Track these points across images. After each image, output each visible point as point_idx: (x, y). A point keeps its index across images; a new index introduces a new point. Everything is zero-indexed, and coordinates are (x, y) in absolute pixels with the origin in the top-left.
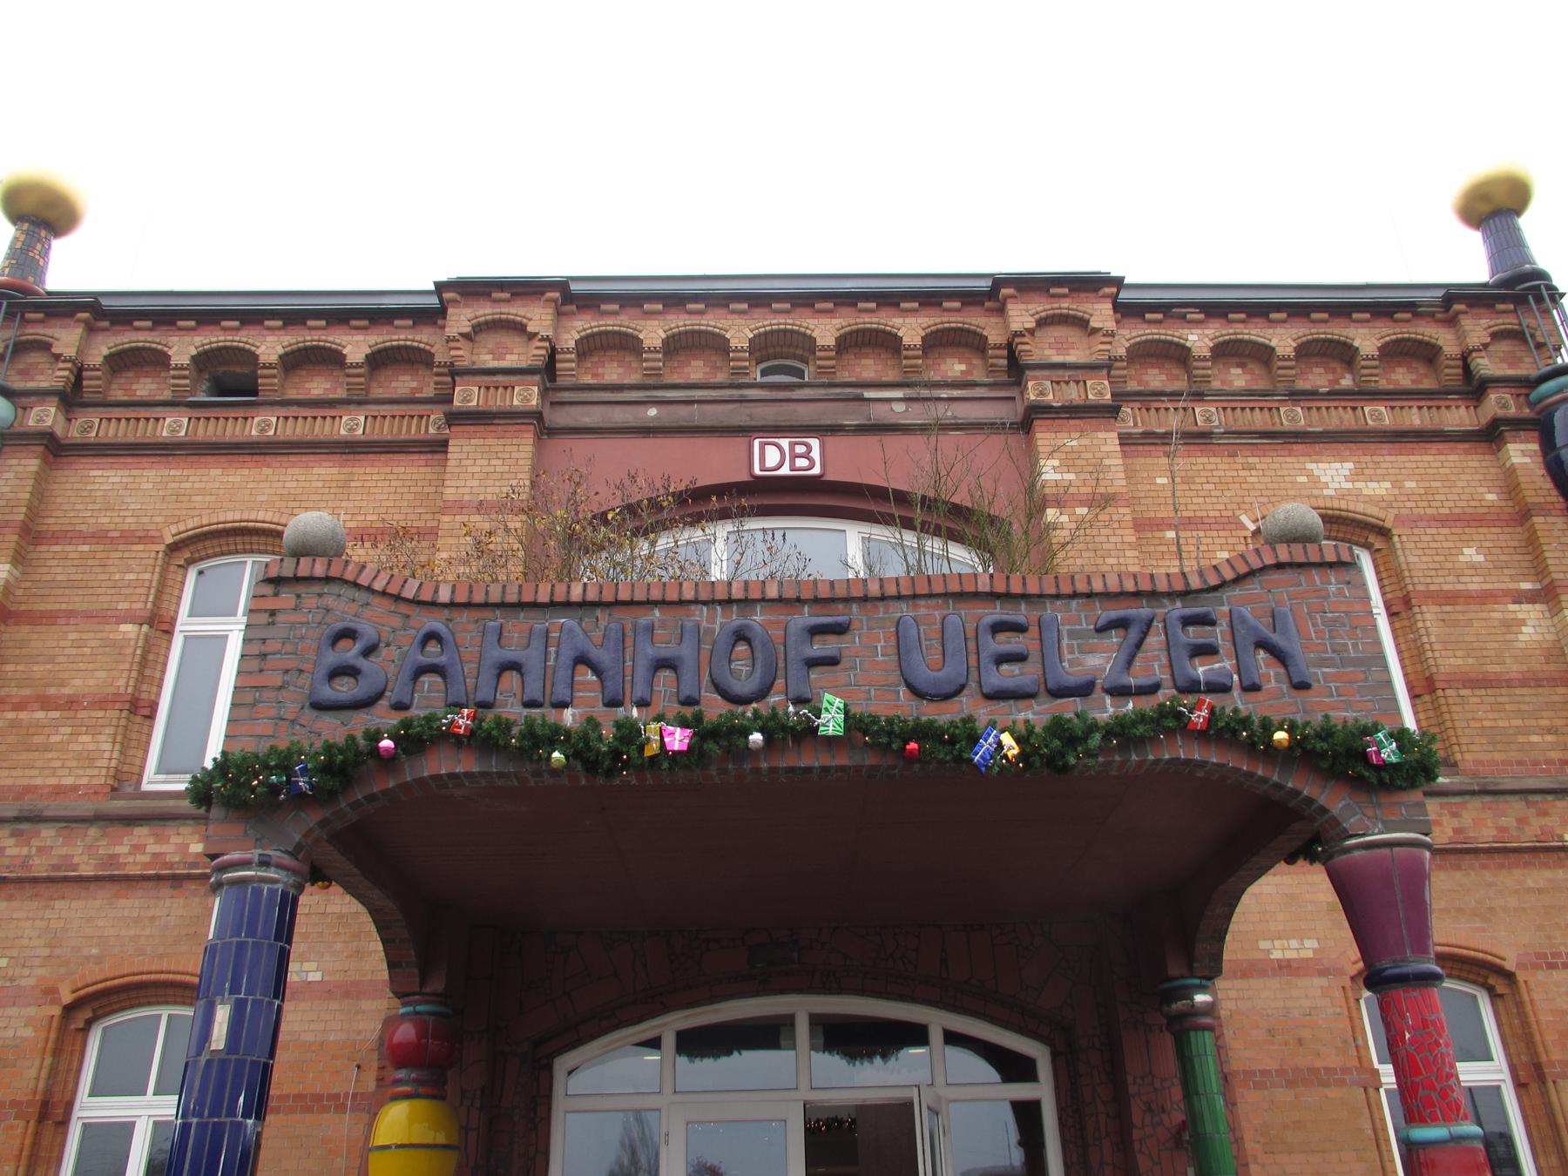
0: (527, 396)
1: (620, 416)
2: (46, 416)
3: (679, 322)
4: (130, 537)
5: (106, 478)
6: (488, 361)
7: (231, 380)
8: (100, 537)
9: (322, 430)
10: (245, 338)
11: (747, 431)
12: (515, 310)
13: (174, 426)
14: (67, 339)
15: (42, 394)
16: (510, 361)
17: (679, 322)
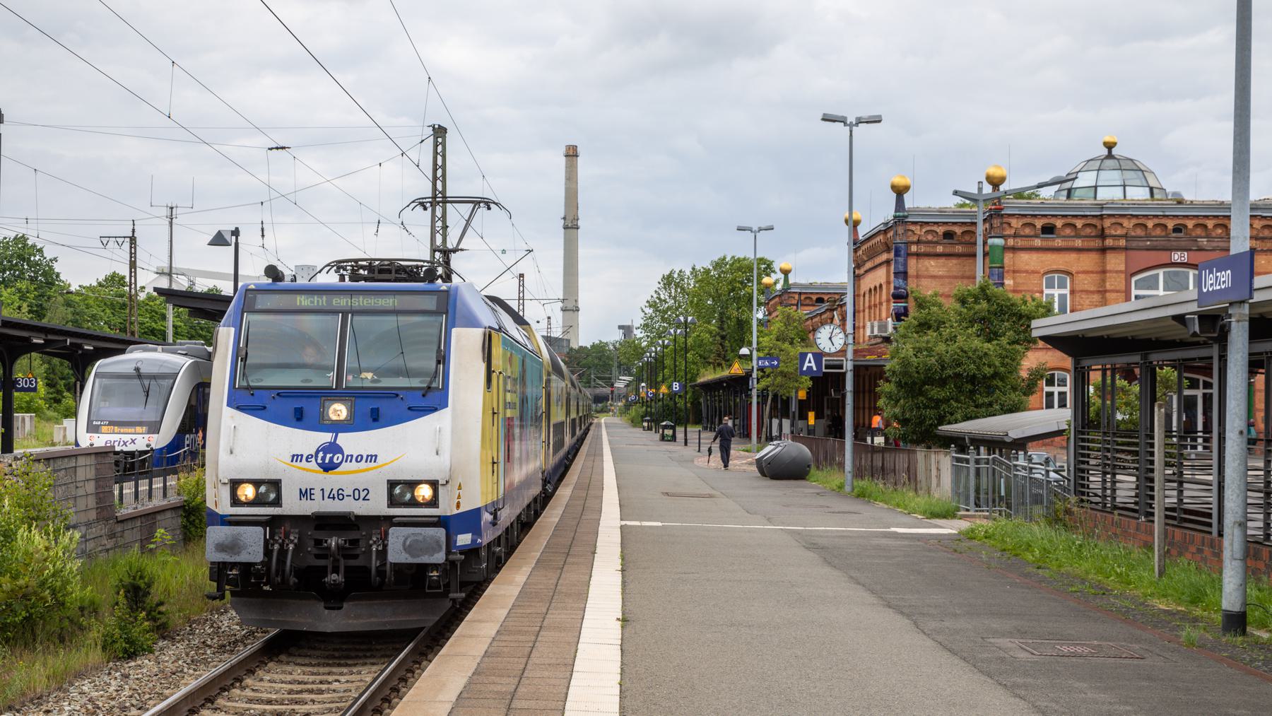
0: (1122, 243)
1: (1141, 244)
2: (1011, 242)
3: (1157, 221)
4: (1034, 272)
5: (1025, 257)
6: (1113, 232)
7: (1048, 230)
8: (1026, 272)
9: (1070, 244)
10: (1052, 221)
11: (1171, 250)
12: (1120, 220)
13: (1037, 242)
14: (1014, 222)
15: (1009, 236)
16: (1119, 232)
17: (1157, 221)
